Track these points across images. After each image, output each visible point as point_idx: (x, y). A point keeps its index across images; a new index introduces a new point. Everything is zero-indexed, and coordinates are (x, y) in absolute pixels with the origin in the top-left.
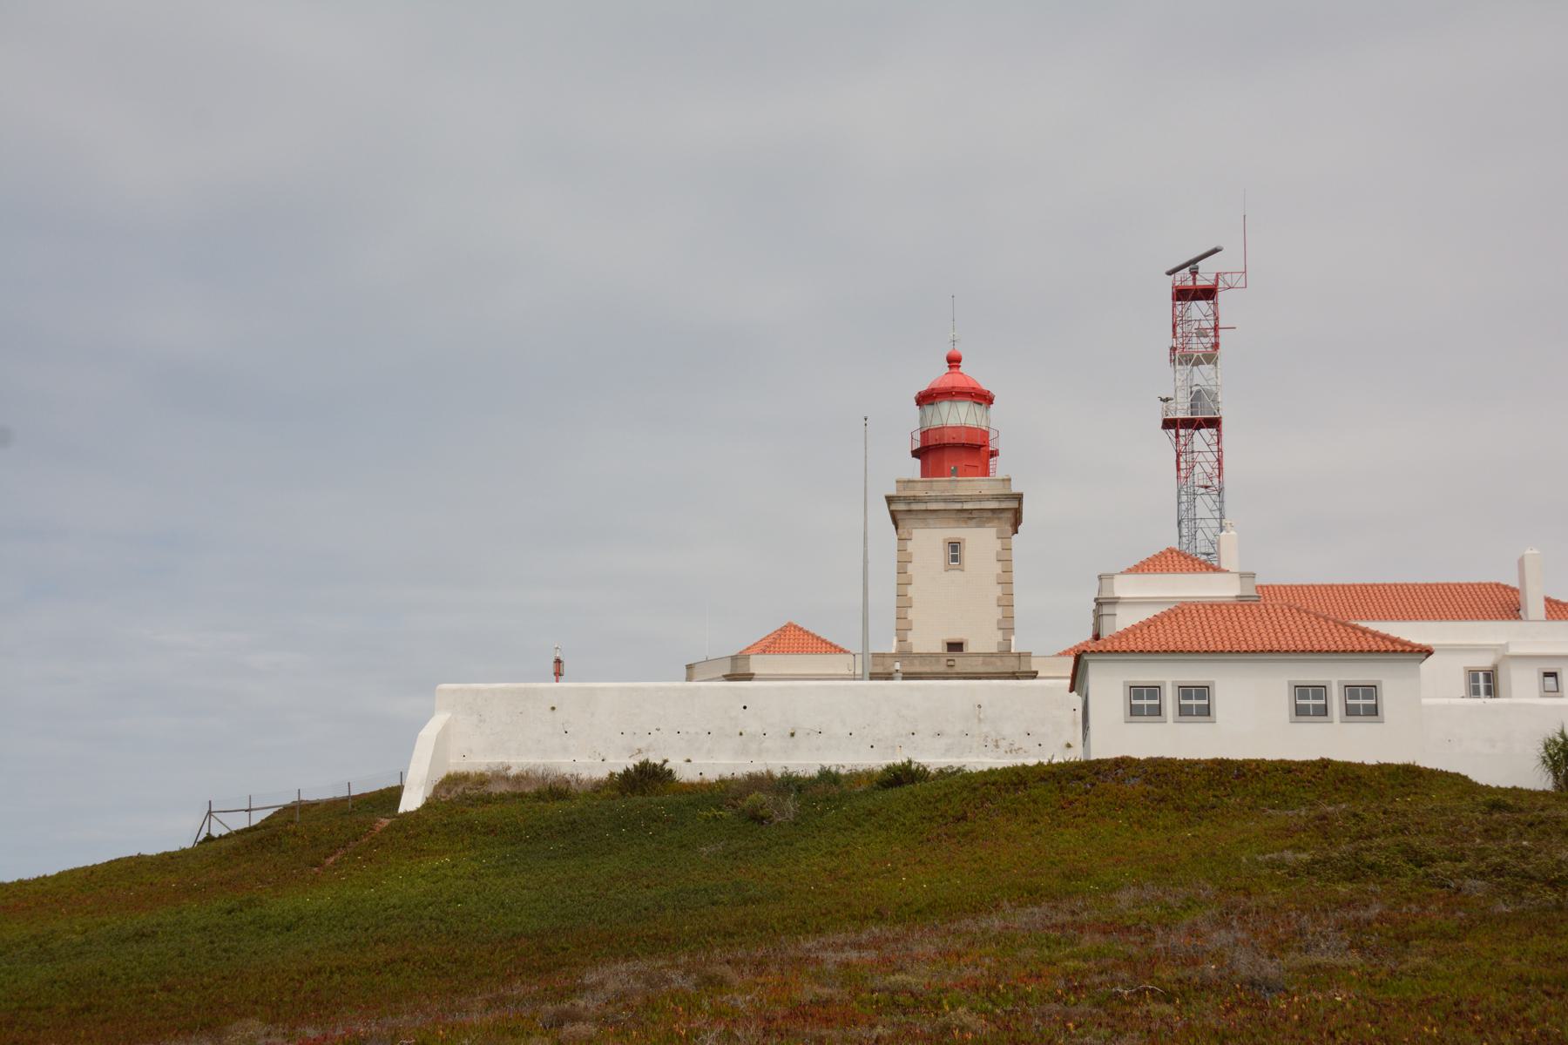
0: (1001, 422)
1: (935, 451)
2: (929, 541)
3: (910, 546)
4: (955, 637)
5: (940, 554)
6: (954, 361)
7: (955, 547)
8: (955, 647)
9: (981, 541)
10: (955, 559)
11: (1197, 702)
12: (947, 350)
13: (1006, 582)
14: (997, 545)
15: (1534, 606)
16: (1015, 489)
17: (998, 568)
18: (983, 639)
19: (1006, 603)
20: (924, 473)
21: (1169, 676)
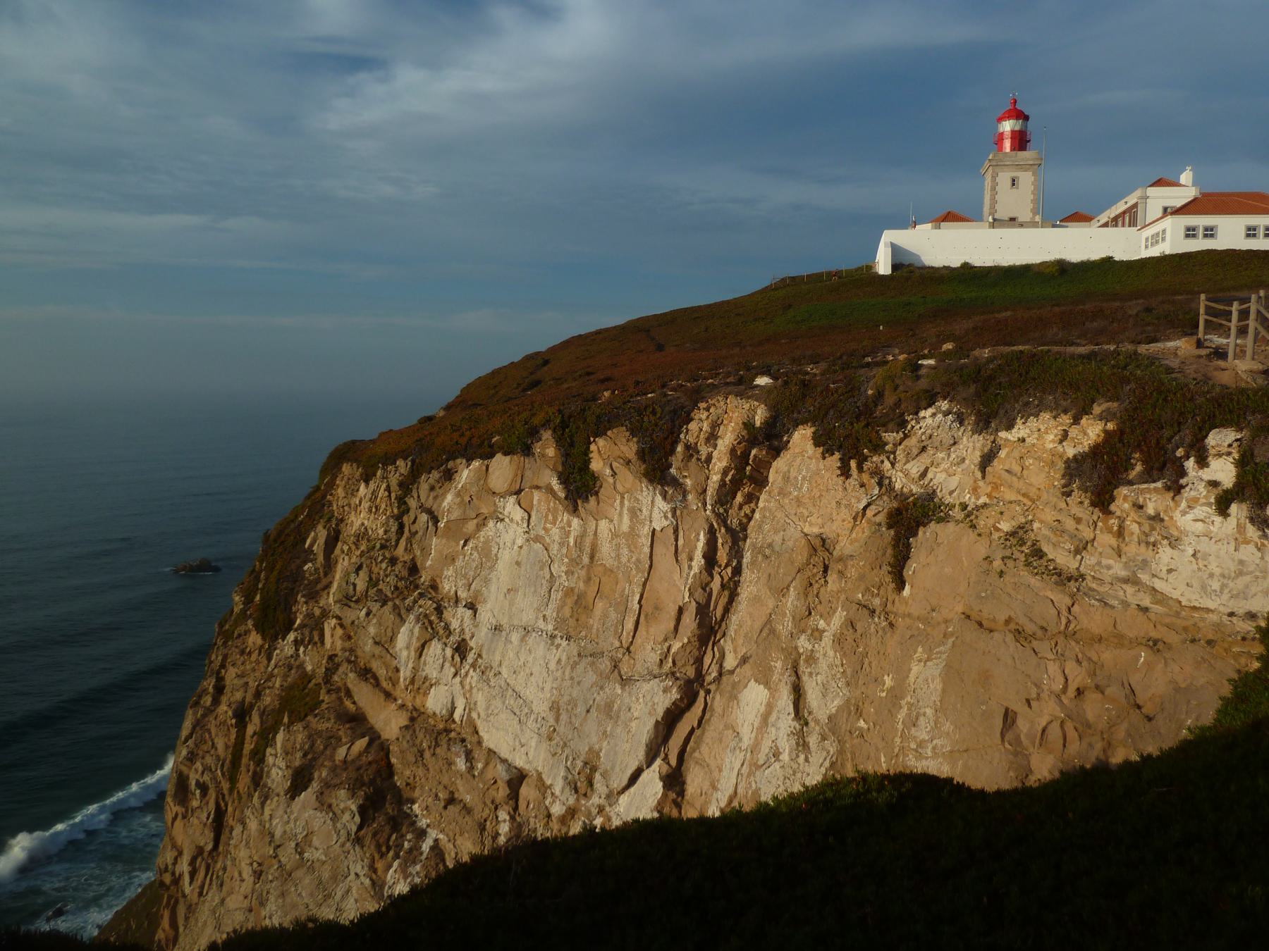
2: (1004, 178)
5: (1010, 183)
7: (1014, 182)
8: (1013, 219)
9: (1026, 179)
11: (1210, 232)
18: (1025, 216)
21: (1201, 221)
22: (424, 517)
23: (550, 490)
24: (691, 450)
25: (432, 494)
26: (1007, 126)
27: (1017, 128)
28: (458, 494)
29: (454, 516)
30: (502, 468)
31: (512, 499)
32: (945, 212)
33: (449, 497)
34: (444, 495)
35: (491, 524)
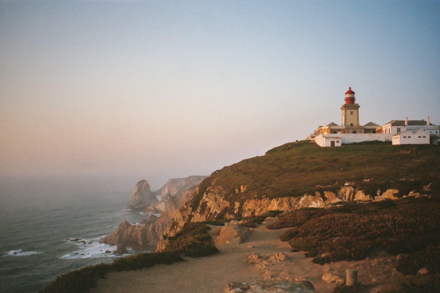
0: (356, 96)
1: (347, 100)
2: (349, 112)
3: (347, 112)
4: (351, 123)
6: (350, 88)
7: (352, 113)
9: (355, 111)
10: (351, 114)
12: (349, 87)
13: (358, 116)
14: (357, 112)
15: (428, 124)
16: (359, 105)
17: (357, 115)
18: (355, 124)
19: (358, 119)
20: (346, 102)
22: (297, 205)
23: (321, 200)
24: (343, 194)
25: (296, 202)
26: (348, 96)
27: (351, 96)
28: (302, 201)
29: (303, 205)
30: (310, 197)
31: (314, 202)
32: (331, 122)
33: (301, 202)
34: (300, 202)
35: (310, 205)
